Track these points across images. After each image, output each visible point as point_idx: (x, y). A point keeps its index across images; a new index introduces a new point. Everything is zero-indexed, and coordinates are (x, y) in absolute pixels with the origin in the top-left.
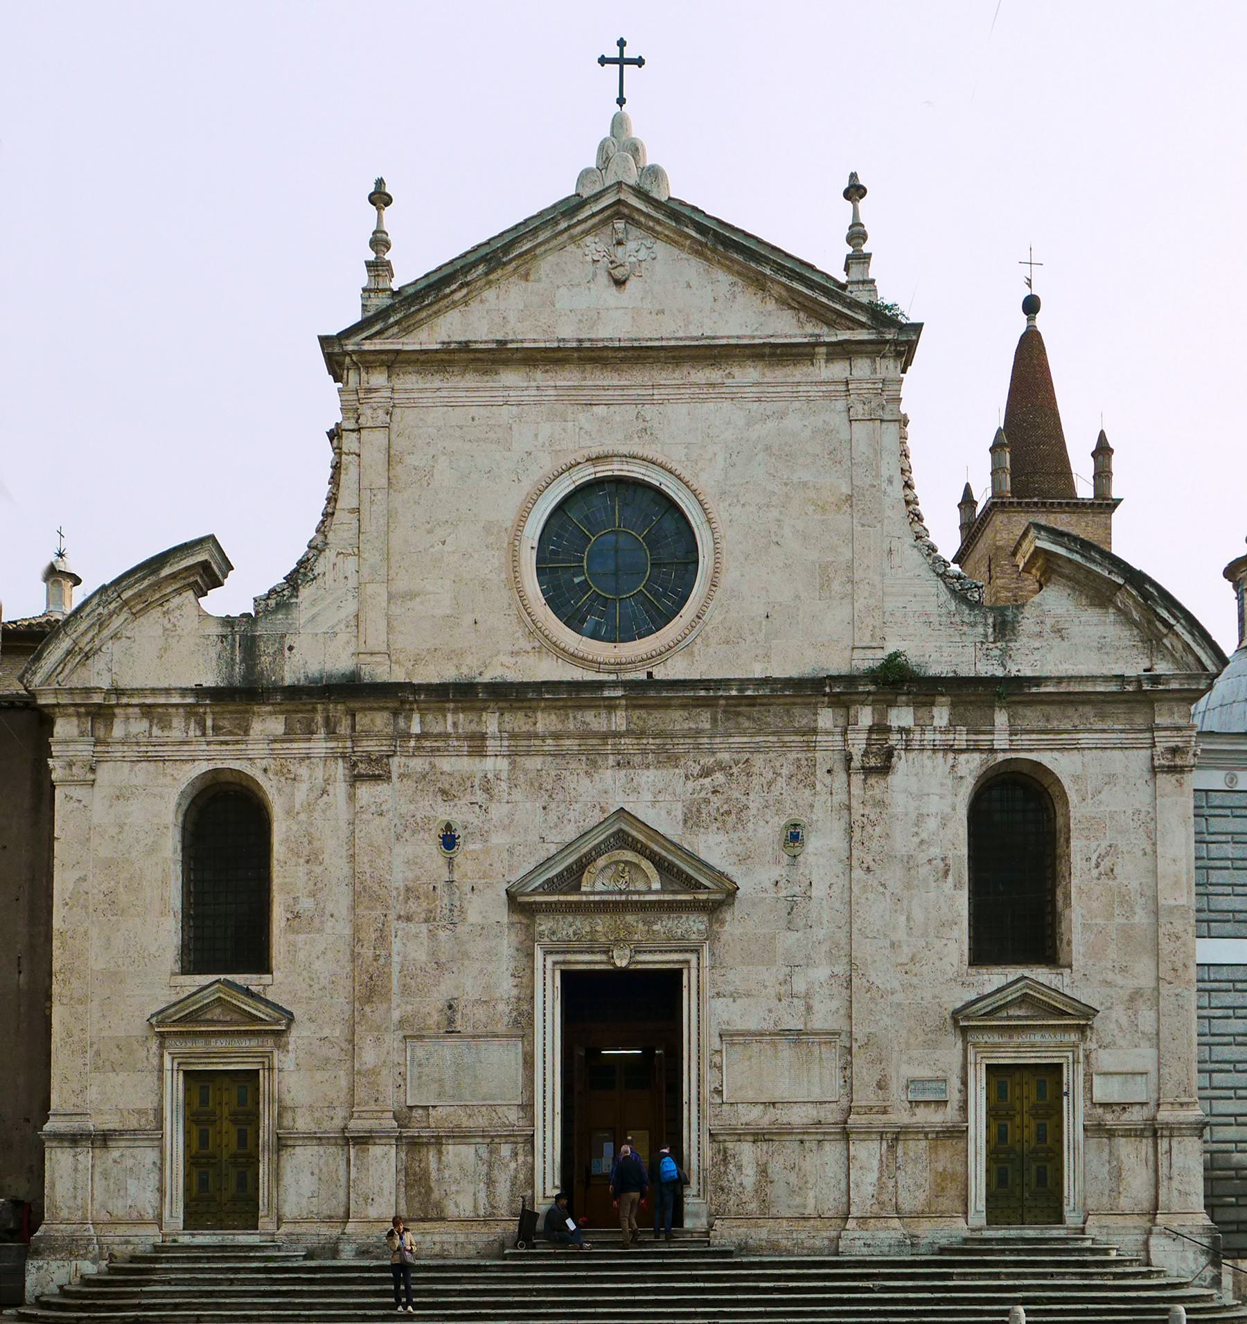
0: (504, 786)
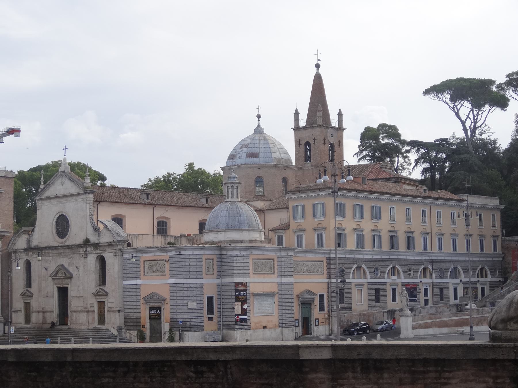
0: (52, 261)
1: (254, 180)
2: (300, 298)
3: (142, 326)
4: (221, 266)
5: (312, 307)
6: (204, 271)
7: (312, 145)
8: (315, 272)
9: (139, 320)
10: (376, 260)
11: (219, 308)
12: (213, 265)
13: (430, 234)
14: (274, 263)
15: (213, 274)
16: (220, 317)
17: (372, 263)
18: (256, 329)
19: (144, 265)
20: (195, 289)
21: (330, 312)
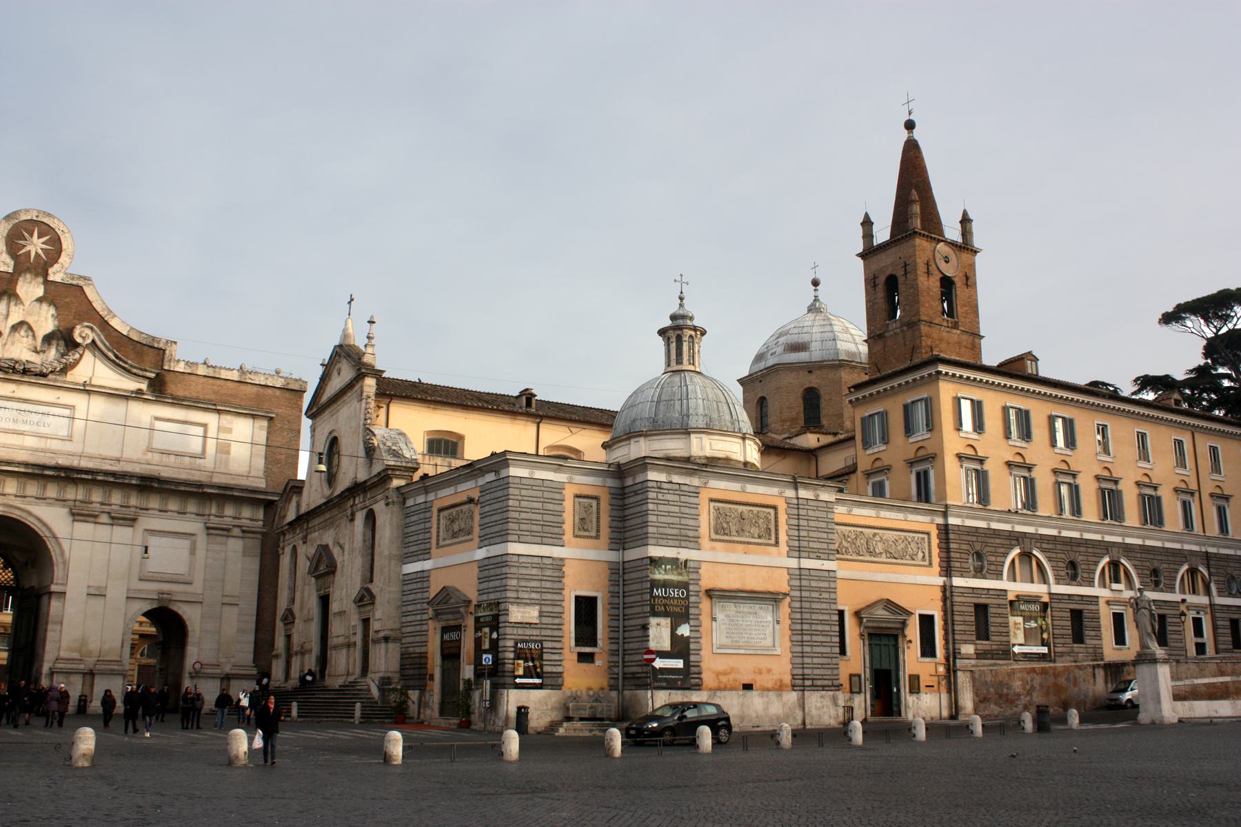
1: (799, 394)
2: (865, 620)
3: (428, 677)
4: (623, 519)
5: (900, 645)
6: (568, 527)
7: (901, 280)
8: (908, 557)
9: (423, 661)
10: (1070, 542)
11: (613, 629)
12: (598, 513)
13: (1197, 494)
14: (776, 518)
15: (597, 537)
16: (618, 655)
17: (1059, 547)
18: (719, 689)
19: (439, 520)
20: (534, 571)
21: (951, 659)
